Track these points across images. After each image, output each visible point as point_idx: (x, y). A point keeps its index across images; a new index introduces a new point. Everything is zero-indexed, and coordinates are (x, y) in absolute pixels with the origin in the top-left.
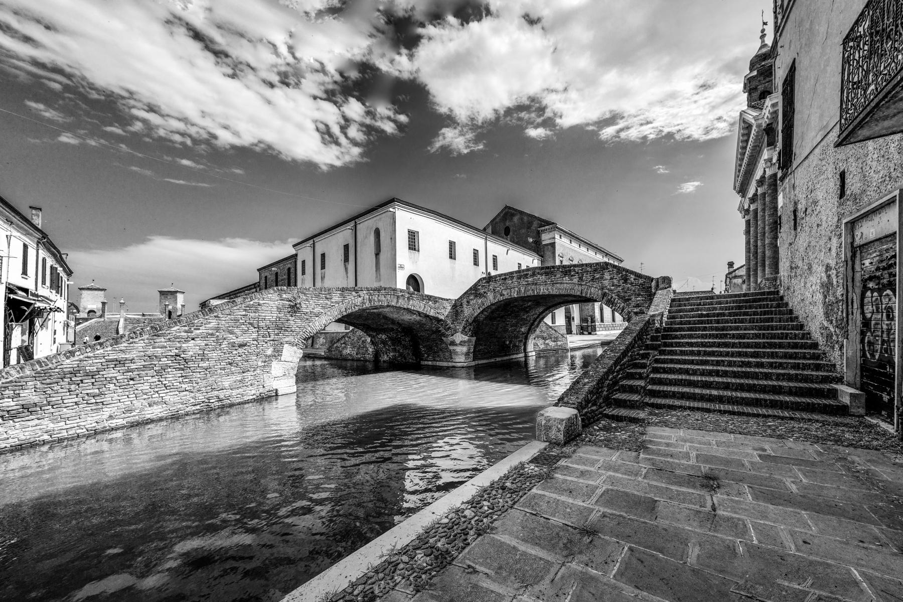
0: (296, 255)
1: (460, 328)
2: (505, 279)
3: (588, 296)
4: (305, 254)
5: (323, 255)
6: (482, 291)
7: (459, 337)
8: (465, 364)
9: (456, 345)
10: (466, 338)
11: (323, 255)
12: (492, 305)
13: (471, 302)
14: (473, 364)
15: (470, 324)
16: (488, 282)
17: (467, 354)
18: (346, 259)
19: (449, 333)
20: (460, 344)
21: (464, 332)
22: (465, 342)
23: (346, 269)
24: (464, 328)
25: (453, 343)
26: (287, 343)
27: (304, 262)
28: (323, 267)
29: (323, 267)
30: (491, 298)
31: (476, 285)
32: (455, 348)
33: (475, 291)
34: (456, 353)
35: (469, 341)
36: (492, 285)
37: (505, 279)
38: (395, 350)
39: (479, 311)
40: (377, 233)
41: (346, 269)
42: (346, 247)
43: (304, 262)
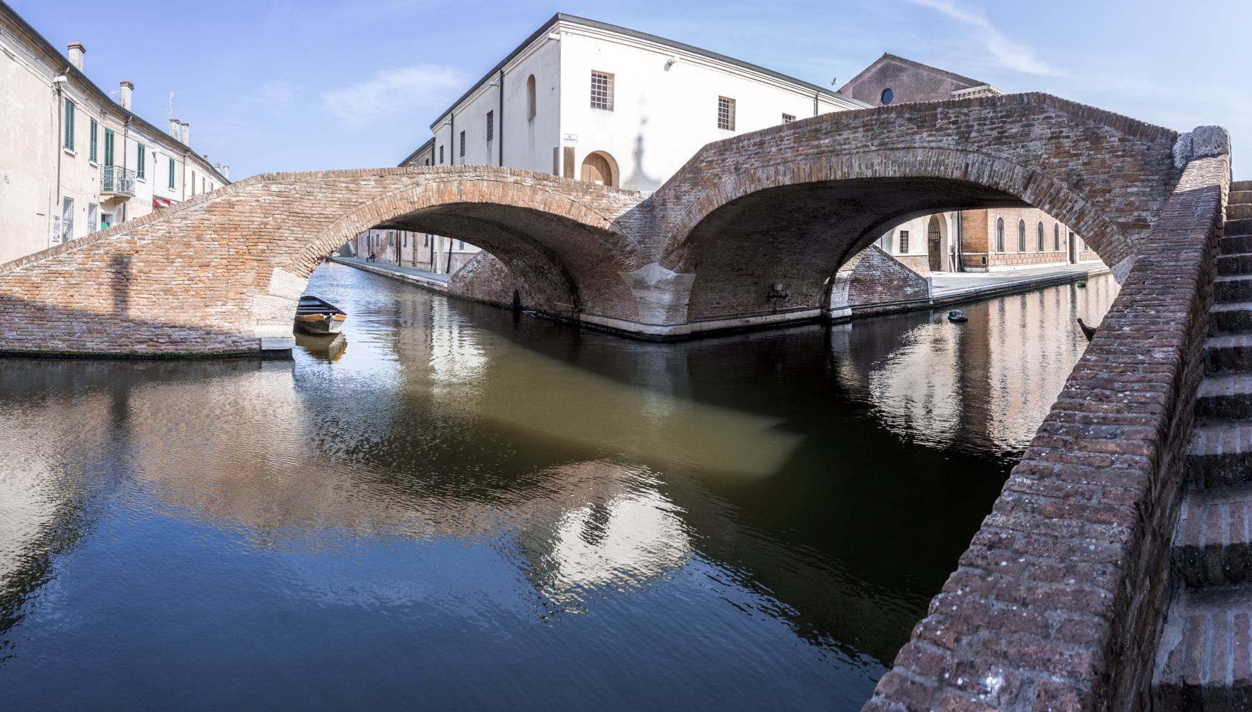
0: (434, 139)
1: (658, 254)
2: (762, 144)
3: (972, 179)
4: (443, 139)
5: (463, 134)
6: (707, 174)
7: (658, 273)
8: (665, 331)
9: (647, 288)
10: (671, 274)
11: (463, 134)
12: (733, 203)
13: (685, 199)
14: (686, 329)
15: (684, 244)
16: (721, 153)
17: (672, 309)
18: (490, 137)
19: (632, 261)
20: (657, 287)
21: (666, 262)
22: (668, 282)
23: (489, 150)
24: (668, 253)
25: (641, 284)
26: (278, 264)
27: (442, 148)
28: (462, 154)
29: (462, 154)
30: (729, 188)
31: (696, 158)
32: (645, 294)
33: (693, 172)
34: (647, 305)
35: (676, 282)
36: (731, 160)
37: (762, 144)
38: (540, 290)
39: (699, 218)
40: (532, 80)
41: (489, 150)
42: (490, 115)
43: (442, 148)
